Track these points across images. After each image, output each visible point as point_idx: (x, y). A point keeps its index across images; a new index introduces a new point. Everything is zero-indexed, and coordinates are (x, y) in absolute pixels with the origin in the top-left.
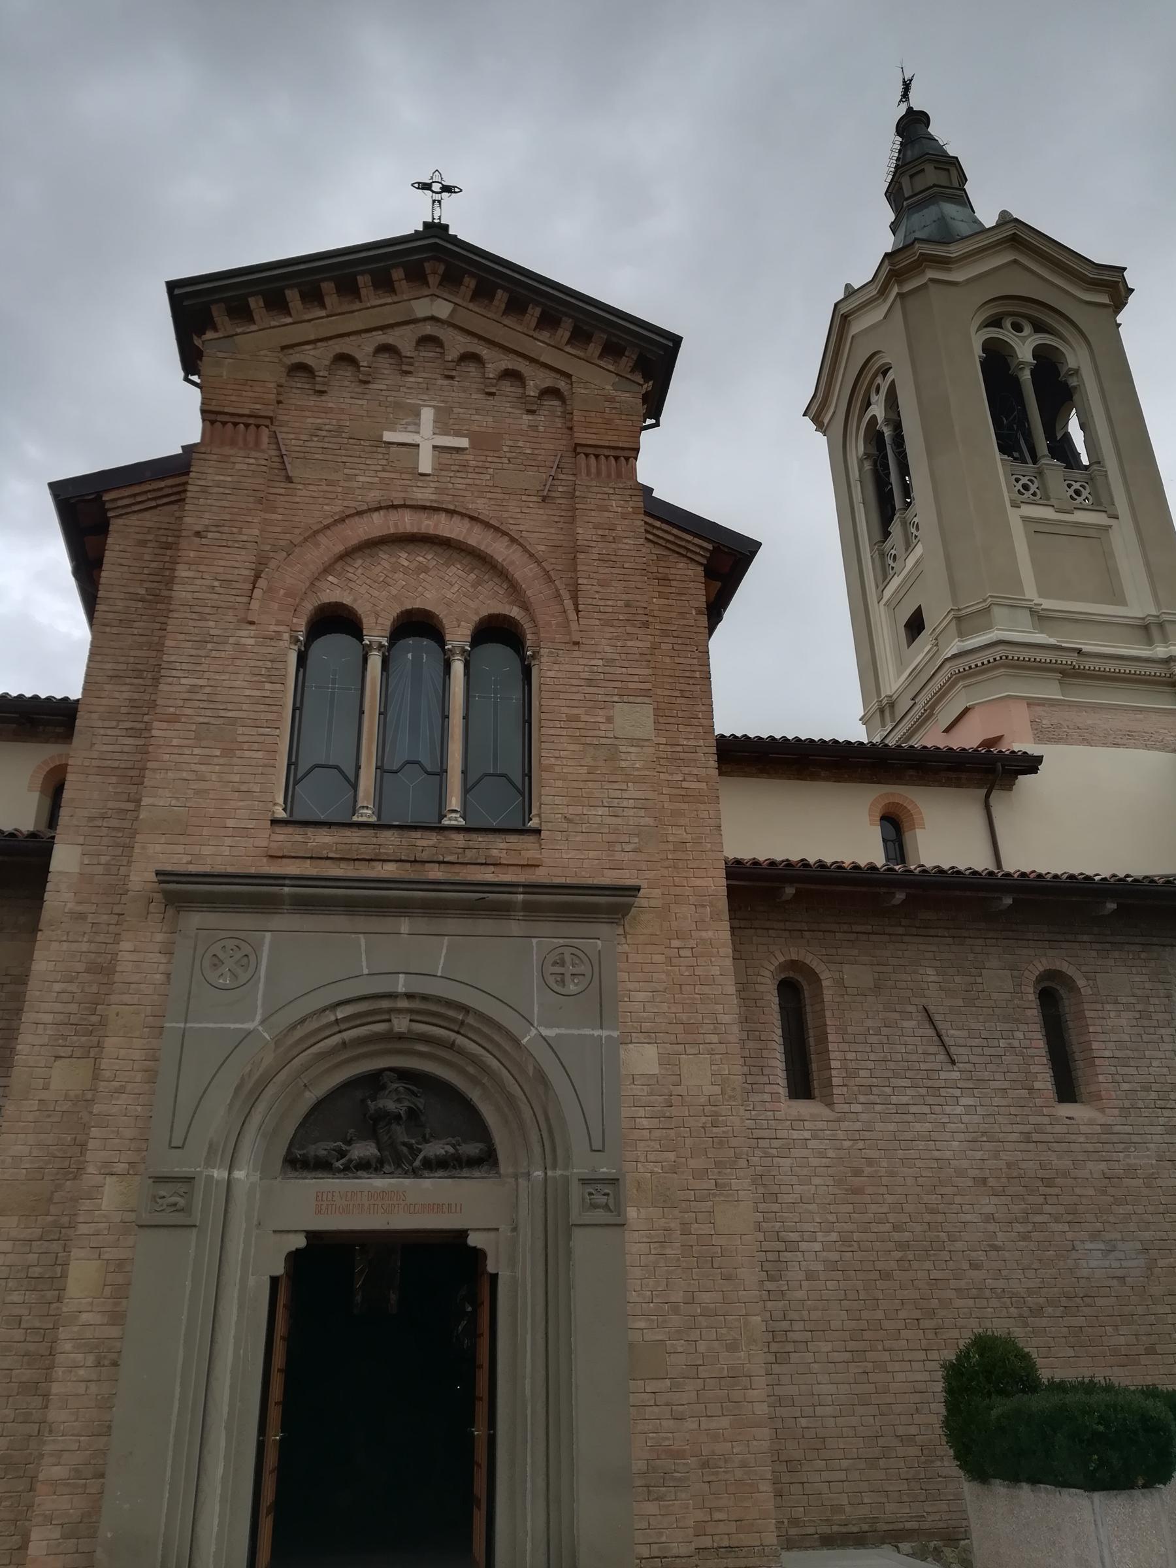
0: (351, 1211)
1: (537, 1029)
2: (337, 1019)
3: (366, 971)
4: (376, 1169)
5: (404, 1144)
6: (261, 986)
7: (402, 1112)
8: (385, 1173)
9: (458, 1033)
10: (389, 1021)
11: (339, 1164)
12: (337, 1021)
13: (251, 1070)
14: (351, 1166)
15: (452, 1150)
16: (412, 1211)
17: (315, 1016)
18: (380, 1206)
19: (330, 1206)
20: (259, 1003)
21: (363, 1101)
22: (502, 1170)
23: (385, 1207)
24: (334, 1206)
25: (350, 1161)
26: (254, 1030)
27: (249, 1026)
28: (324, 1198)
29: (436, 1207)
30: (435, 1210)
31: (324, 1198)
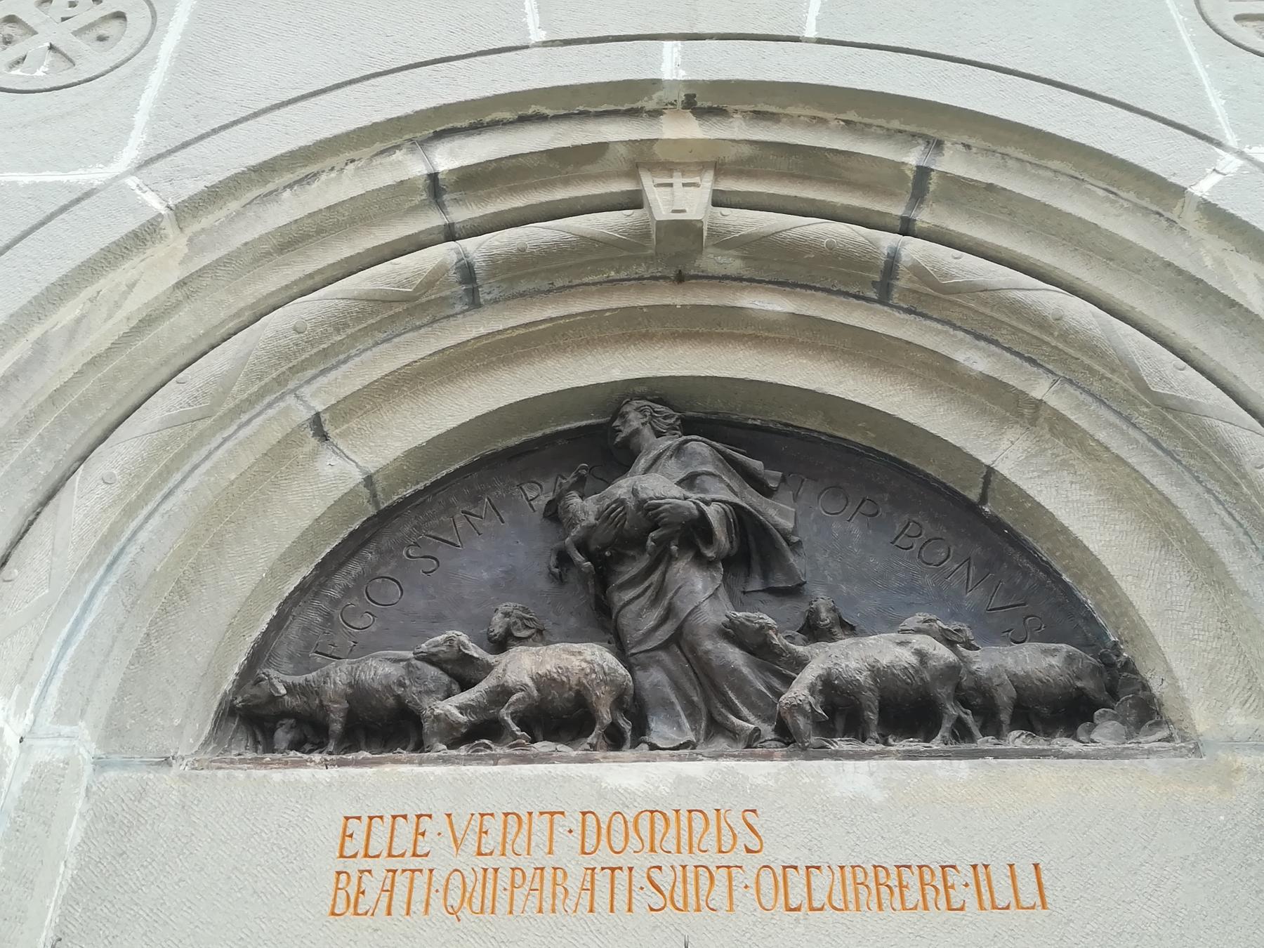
0: (503, 897)
1: (1241, 154)
2: (433, 177)
3: (538, 35)
4: (615, 740)
5: (733, 633)
6: (156, 79)
7: (712, 512)
8: (653, 747)
9: (906, 228)
10: (634, 201)
11: (451, 707)
12: (435, 186)
13: (78, 321)
14: (505, 714)
15: (942, 653)
16: (798, 895)
17: (351, 166)
18: (640, 878)
19: (402, 881)
20: (140, 119)
21: (555, 513)
22: (1201, 719)
23: (665, 880)
24: (421, 880)
25: (502, 694)
26: (106, 185)
27: (95, 175)
28: (379, 844)
29: (911, 879)
30: (913, 896)
31: (379, 844)
